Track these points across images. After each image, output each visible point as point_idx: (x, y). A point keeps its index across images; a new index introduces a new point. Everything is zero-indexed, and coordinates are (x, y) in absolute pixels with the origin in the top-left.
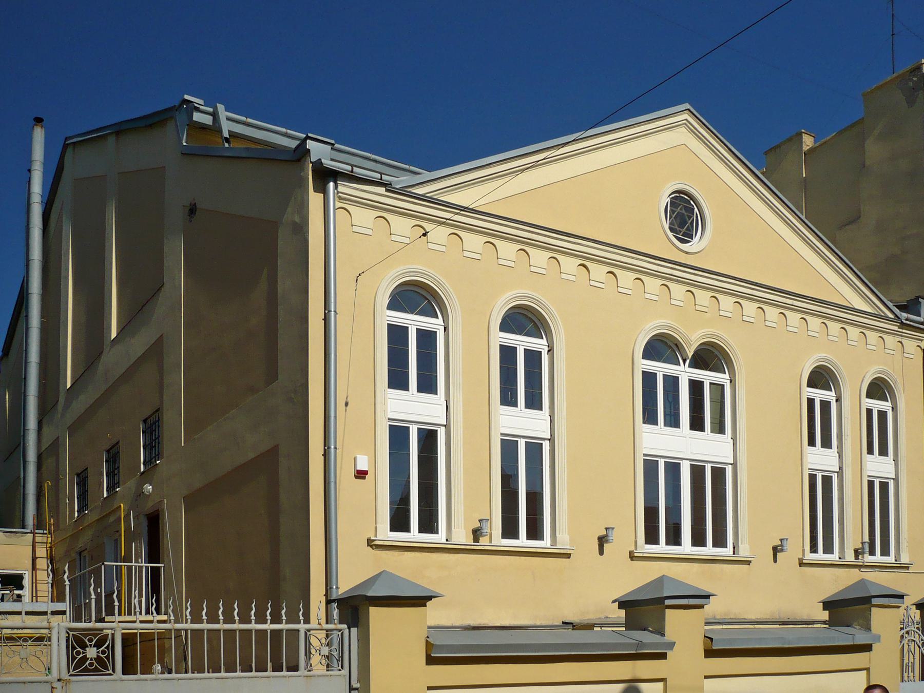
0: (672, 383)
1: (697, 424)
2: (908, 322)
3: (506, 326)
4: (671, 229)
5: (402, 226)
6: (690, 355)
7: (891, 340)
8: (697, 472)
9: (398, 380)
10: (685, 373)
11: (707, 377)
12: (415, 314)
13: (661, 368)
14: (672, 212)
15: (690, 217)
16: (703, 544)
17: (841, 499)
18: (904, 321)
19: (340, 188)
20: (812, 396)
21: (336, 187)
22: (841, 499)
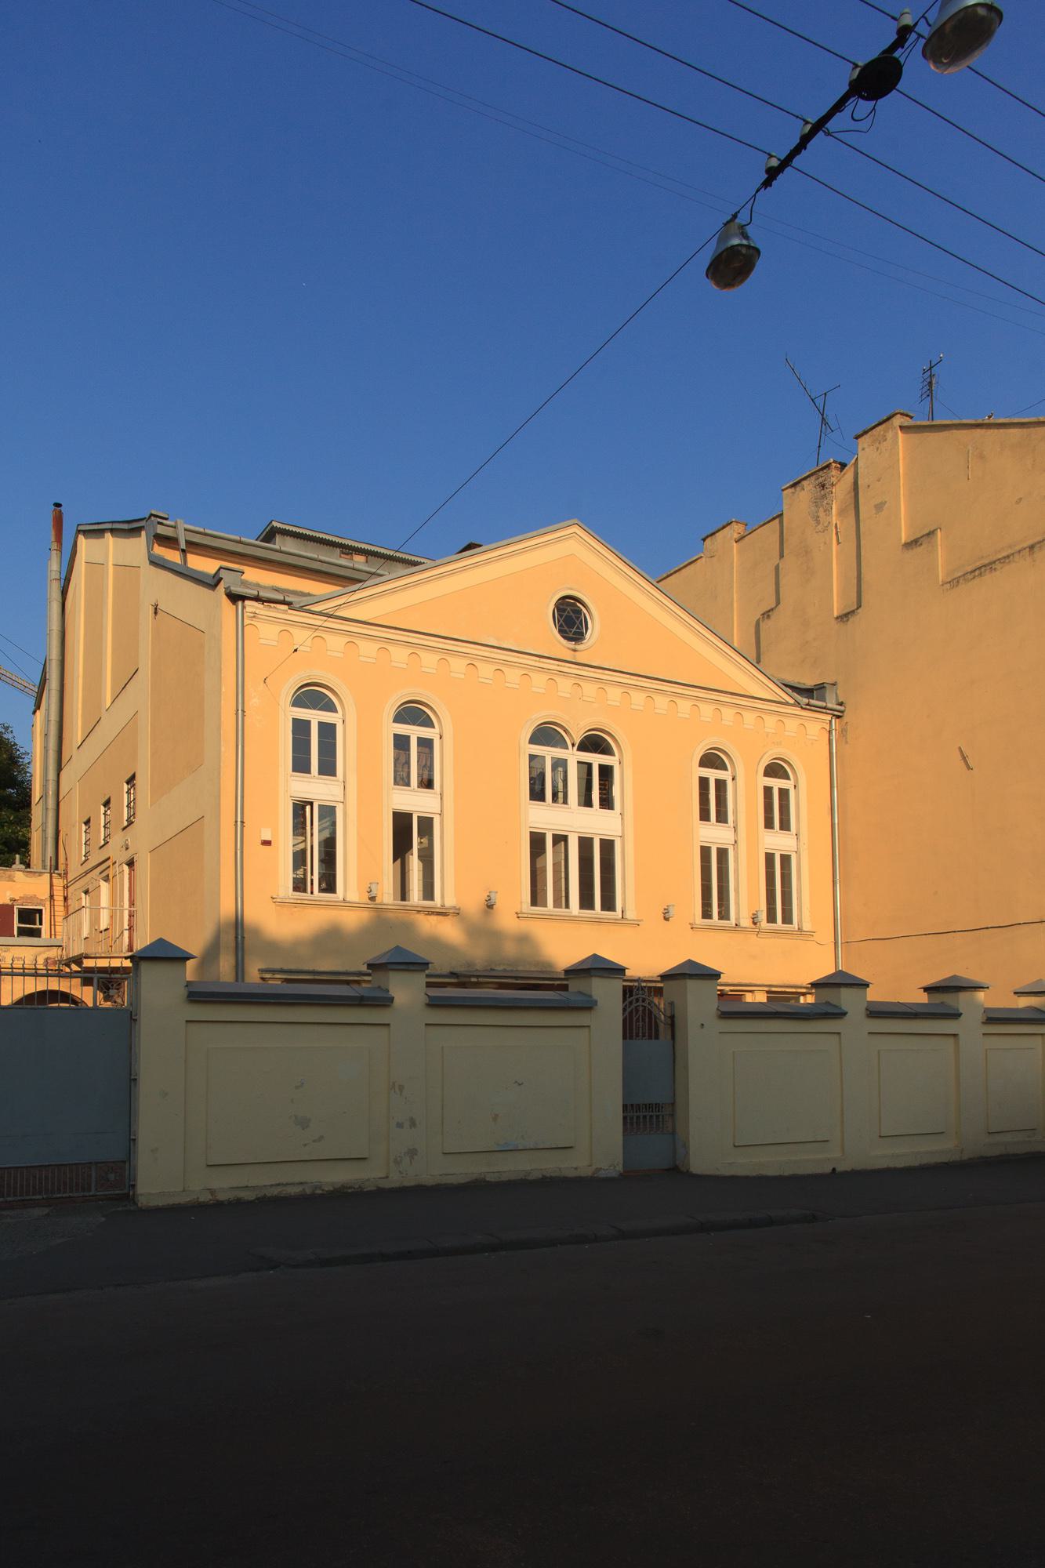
0: (560, 764)
1: (587, 802)
2: (808, 707)
3: (399, 718)
4: (560, 631)
5: (301, 636)
6: (577, 742)
7: (792, 725)
8: (585, 844)
9: (301, 765)
10: (573, 757)
11: (596, 760)
12: (318, 710)
13: (549, 753)
14: (560, 616)
15: (578, 618)
16: (591, 907)
17: (736, 871)
18: (804, 706)
19: (248, 609)
20: (769, 784)
21: (244, 607)
22: (736, 871)
